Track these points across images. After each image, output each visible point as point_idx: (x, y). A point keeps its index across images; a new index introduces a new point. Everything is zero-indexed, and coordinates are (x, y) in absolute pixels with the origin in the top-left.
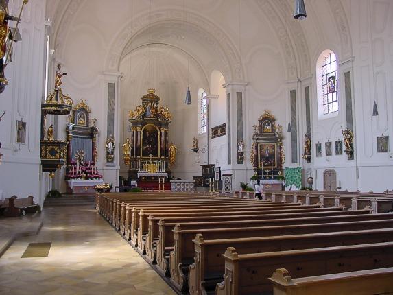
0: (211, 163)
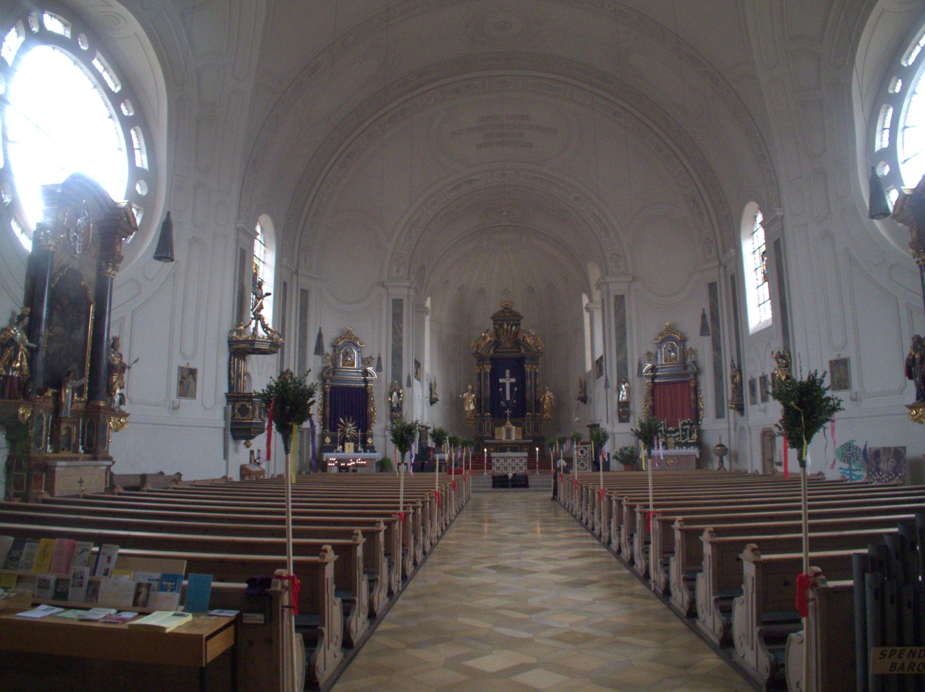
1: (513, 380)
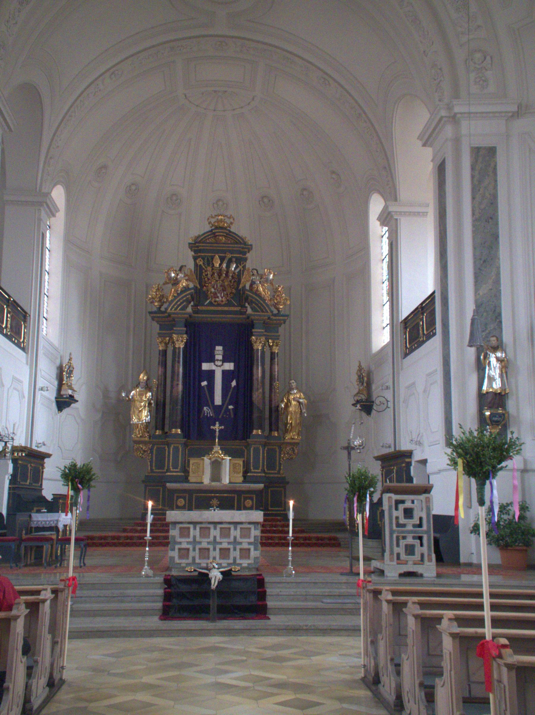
1: (229, 366)
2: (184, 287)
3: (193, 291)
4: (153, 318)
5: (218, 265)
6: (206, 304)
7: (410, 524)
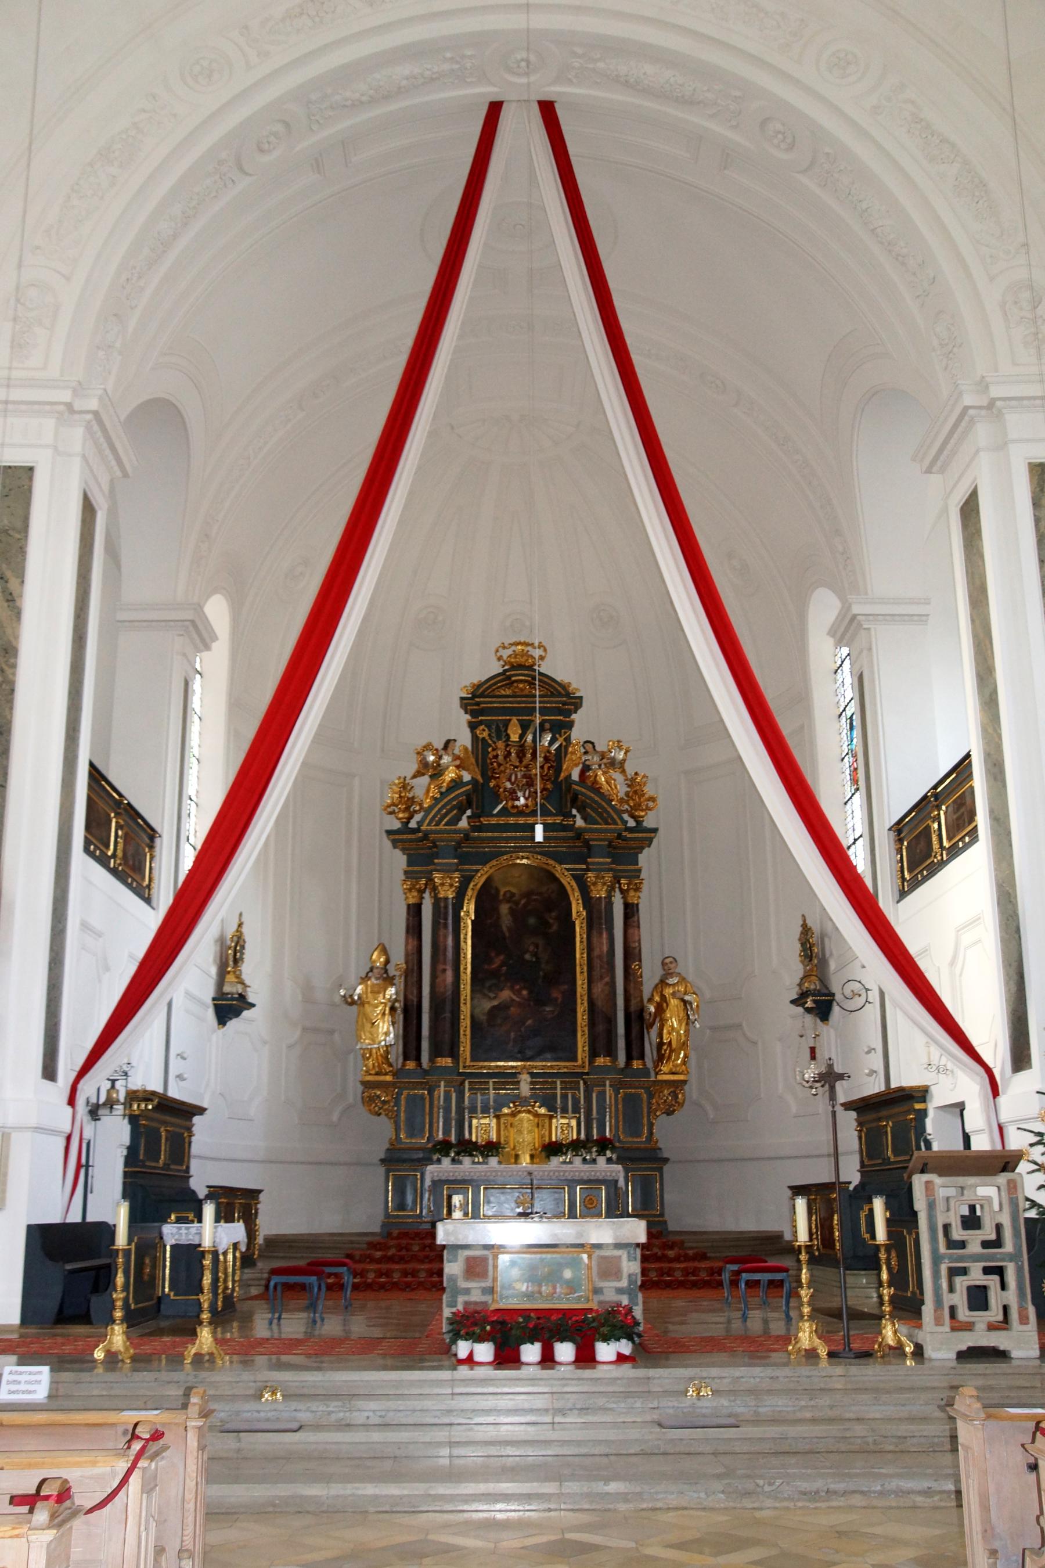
0: (904, 1078)
2: (453, 780)
3: (470, 787)
4: (395, 844)
5: (517, 736)
6: (495, 812)
7: (974, 1240)
